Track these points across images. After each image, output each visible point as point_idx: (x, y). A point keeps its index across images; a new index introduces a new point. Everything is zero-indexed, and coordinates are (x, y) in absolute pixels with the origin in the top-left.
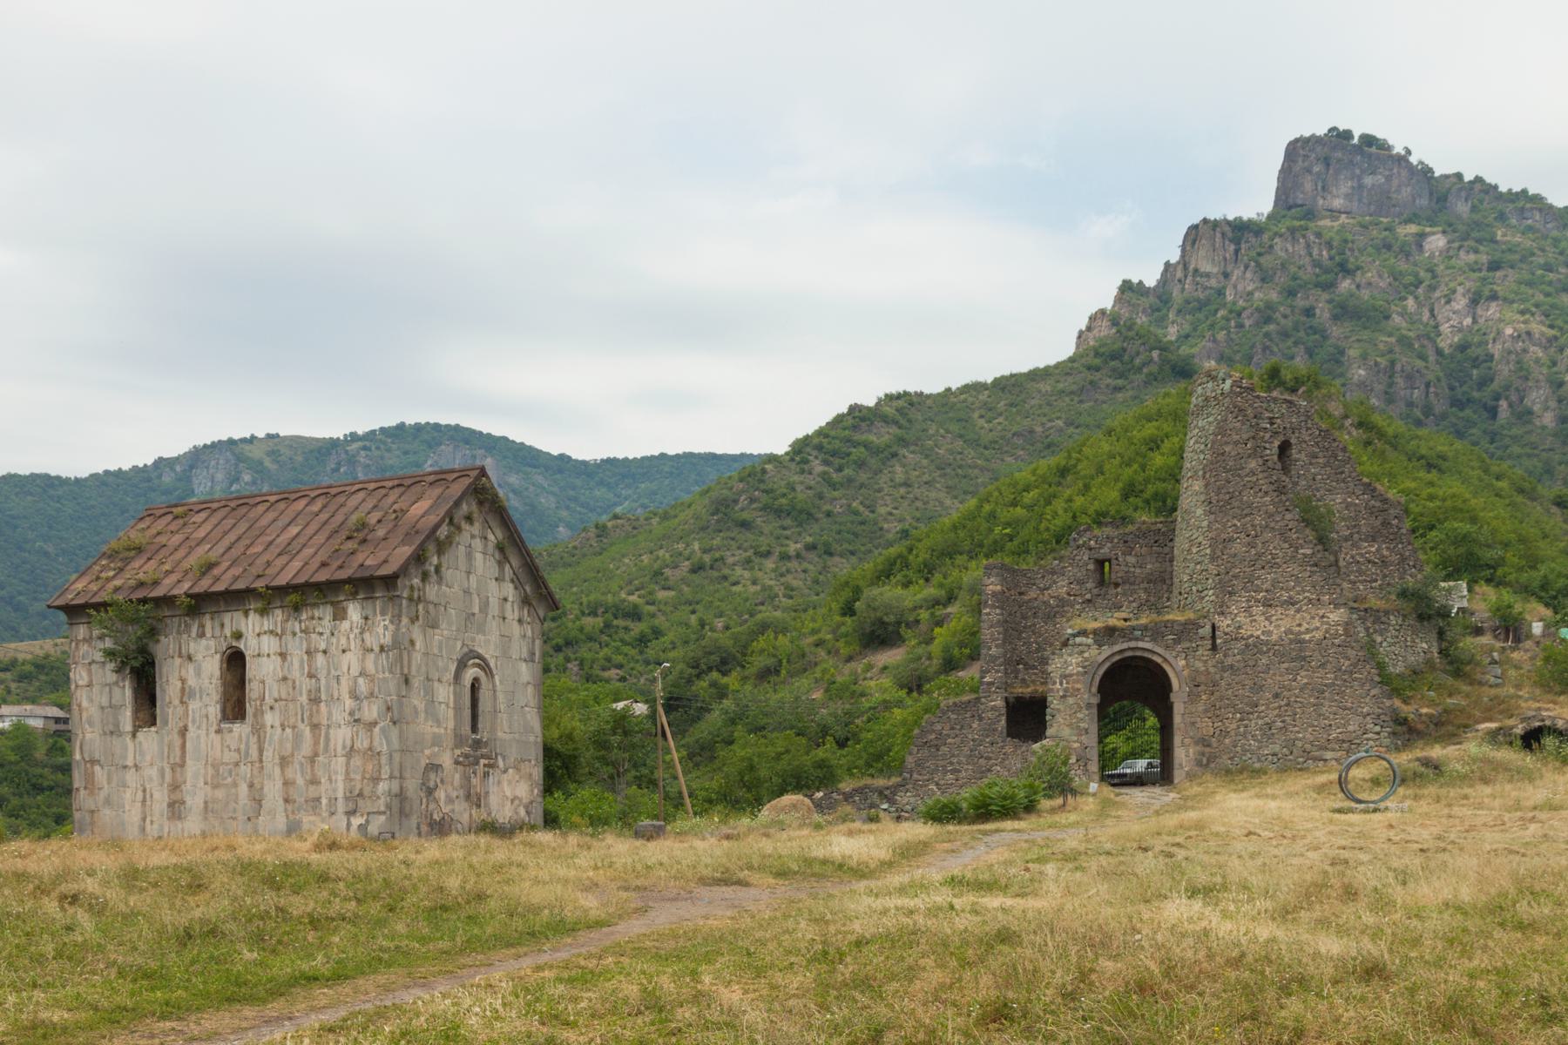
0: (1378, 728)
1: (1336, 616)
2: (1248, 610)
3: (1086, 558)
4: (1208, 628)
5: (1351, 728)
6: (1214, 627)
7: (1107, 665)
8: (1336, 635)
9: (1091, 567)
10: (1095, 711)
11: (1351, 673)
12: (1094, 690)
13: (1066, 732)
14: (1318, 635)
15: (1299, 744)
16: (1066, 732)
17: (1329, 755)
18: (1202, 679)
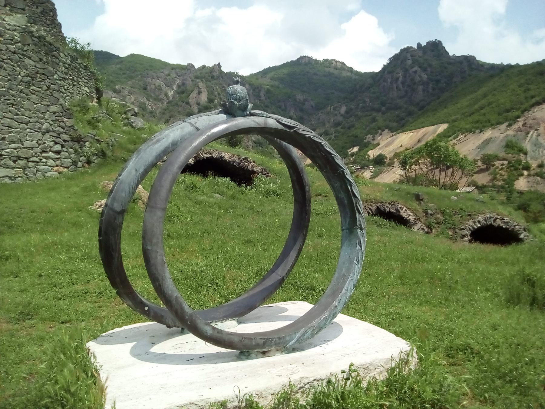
0: (58, 147)
5: (26, 144)
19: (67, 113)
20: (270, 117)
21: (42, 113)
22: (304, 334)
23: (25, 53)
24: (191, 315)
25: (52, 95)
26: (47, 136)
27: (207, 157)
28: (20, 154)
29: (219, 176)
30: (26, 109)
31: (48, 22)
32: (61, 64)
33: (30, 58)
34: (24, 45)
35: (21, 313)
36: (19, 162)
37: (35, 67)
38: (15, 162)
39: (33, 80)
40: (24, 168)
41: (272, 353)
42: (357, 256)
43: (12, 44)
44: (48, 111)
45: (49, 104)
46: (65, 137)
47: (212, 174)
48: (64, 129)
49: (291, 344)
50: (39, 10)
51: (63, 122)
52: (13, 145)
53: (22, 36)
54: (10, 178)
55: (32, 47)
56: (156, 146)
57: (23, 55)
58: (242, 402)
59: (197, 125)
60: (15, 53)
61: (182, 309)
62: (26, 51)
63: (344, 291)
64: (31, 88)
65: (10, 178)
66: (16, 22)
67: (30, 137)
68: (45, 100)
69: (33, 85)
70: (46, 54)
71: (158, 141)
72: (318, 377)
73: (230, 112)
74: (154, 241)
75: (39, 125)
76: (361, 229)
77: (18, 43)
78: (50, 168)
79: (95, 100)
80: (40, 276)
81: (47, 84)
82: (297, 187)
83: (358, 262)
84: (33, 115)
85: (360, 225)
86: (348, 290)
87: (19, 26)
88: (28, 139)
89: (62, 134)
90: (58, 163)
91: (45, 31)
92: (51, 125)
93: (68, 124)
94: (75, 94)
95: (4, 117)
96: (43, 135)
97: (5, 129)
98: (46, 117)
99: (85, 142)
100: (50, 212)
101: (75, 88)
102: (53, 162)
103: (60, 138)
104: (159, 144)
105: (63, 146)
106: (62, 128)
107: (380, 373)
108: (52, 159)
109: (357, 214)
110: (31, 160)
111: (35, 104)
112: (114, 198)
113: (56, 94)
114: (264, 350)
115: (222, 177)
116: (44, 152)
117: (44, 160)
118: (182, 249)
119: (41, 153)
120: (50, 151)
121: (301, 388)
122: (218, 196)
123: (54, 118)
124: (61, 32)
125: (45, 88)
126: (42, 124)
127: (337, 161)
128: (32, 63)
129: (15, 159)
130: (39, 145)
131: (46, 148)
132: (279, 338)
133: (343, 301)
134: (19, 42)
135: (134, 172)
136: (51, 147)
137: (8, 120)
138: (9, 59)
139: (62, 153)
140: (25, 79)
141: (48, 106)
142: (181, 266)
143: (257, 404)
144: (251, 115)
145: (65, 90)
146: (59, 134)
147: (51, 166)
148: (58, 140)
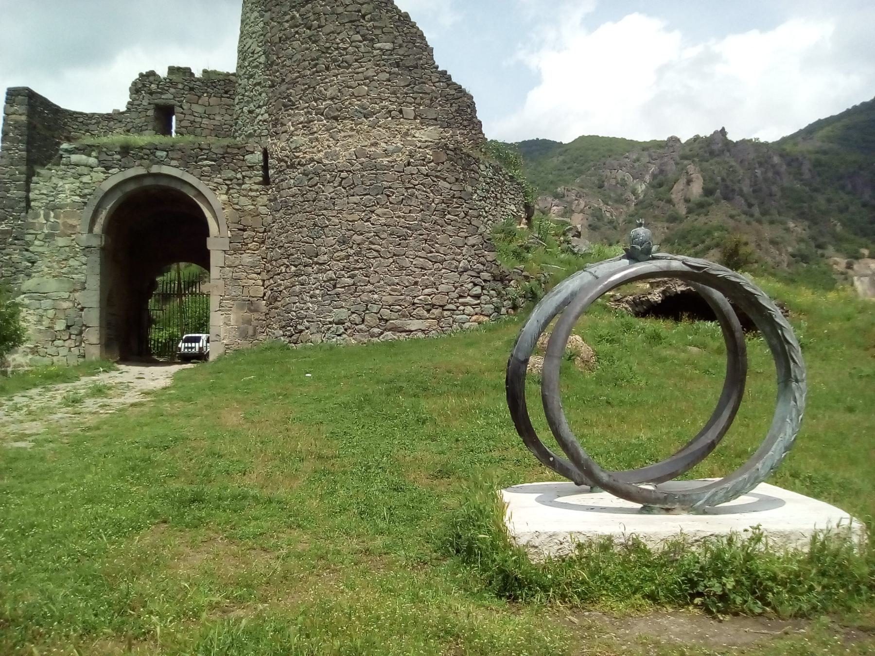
0: (477, 290)
1: (427, 134)
2: (307, 125)
3: (145, 103)
4: (258, 157)
5: (442, 288)
7: (118, 195)
8: (424, 161)
9: (151, 113)
10: (95, 258)
12: (97, 229)
13: (51, 285)
16: (51, 285)
17: (414, 324)
18: (248, 221)
19: (488, 244)
20: (675, 259)
21: (459, 248)
22: (714, 495)
23: (438, 174)
24: (586, 460)
26: (465, 275)
27: (682, 291)
28: (434, 301)
29: (699, 320)
30: (441, 245)
31: (465, 123)
32: (481, 179)
33: (445, 179)
34: (438, 164)
35: (440, 471)
36: (433, 311)
38: (428, 311)
40: (438, 319)
41: (676, 511)
42: (791, 414)
43: (424, 165)
45: (467, 235)
46: (486, 275)
47: (689, 317)
48: (484, 265)
49: (698, 504)
50: (453, 109)
52: (427, 291)
55: (447, 164)
56: (557, 297)
57: (437, 177)
58: (629, 540)
59: (596, 274)
60: (427, 175)
61: (578, 453)
63: (770, 453)
65: (423, 331)
66: (428, 137)
69: (449, 213)
70: (464, 169)
71: (558, 292)
72: (717, 533)
73: (633, 256)
74: (552, 387)
75: (455, 263)
76: (797, 381)
79: (524, 221)
80: (457, 440)
82: (727, 334)
83: (791, 420)
84: (449, 251)
85: (795, 376)
86: (776, 452)
88: (444, 281)
90: (478, 310)
91: (462, 134)
92: (469, 262)
94: (499, 216)
98: (464, 252)
99: (510, 281)
100: (468, 372)
101: (499, 208)
104: (559, 295)
105: (483, 288)
107: (803, 545)
108: (471, 305)
109: (792, 364)
110: (446, 308)
112: (518, 348)
113: (475, 222)
114: (667, 506)
115: (705, 320)
116: (461, 296)
117: (461, 308)
118: (623, 419)
119: (458, 298)
121: (697, 541)
122: (695, 349)
123: (473, 252)
124: (481, 132)
125: (462, 214)
126: (459, 262)
127: (761, 302)
128: (449, 186)
129: (429, 307)
130: (456, 288)
131: (464, 292)
132: (684, 496)
133: (769, 463)
134: (433, 161)
135: (536, 322)
139: (482, 297)
141: (466, 237)
142: (616, 439)
143: (645, 546)
144: (654, 258)
146: (479, 273)
148: (477, 280)
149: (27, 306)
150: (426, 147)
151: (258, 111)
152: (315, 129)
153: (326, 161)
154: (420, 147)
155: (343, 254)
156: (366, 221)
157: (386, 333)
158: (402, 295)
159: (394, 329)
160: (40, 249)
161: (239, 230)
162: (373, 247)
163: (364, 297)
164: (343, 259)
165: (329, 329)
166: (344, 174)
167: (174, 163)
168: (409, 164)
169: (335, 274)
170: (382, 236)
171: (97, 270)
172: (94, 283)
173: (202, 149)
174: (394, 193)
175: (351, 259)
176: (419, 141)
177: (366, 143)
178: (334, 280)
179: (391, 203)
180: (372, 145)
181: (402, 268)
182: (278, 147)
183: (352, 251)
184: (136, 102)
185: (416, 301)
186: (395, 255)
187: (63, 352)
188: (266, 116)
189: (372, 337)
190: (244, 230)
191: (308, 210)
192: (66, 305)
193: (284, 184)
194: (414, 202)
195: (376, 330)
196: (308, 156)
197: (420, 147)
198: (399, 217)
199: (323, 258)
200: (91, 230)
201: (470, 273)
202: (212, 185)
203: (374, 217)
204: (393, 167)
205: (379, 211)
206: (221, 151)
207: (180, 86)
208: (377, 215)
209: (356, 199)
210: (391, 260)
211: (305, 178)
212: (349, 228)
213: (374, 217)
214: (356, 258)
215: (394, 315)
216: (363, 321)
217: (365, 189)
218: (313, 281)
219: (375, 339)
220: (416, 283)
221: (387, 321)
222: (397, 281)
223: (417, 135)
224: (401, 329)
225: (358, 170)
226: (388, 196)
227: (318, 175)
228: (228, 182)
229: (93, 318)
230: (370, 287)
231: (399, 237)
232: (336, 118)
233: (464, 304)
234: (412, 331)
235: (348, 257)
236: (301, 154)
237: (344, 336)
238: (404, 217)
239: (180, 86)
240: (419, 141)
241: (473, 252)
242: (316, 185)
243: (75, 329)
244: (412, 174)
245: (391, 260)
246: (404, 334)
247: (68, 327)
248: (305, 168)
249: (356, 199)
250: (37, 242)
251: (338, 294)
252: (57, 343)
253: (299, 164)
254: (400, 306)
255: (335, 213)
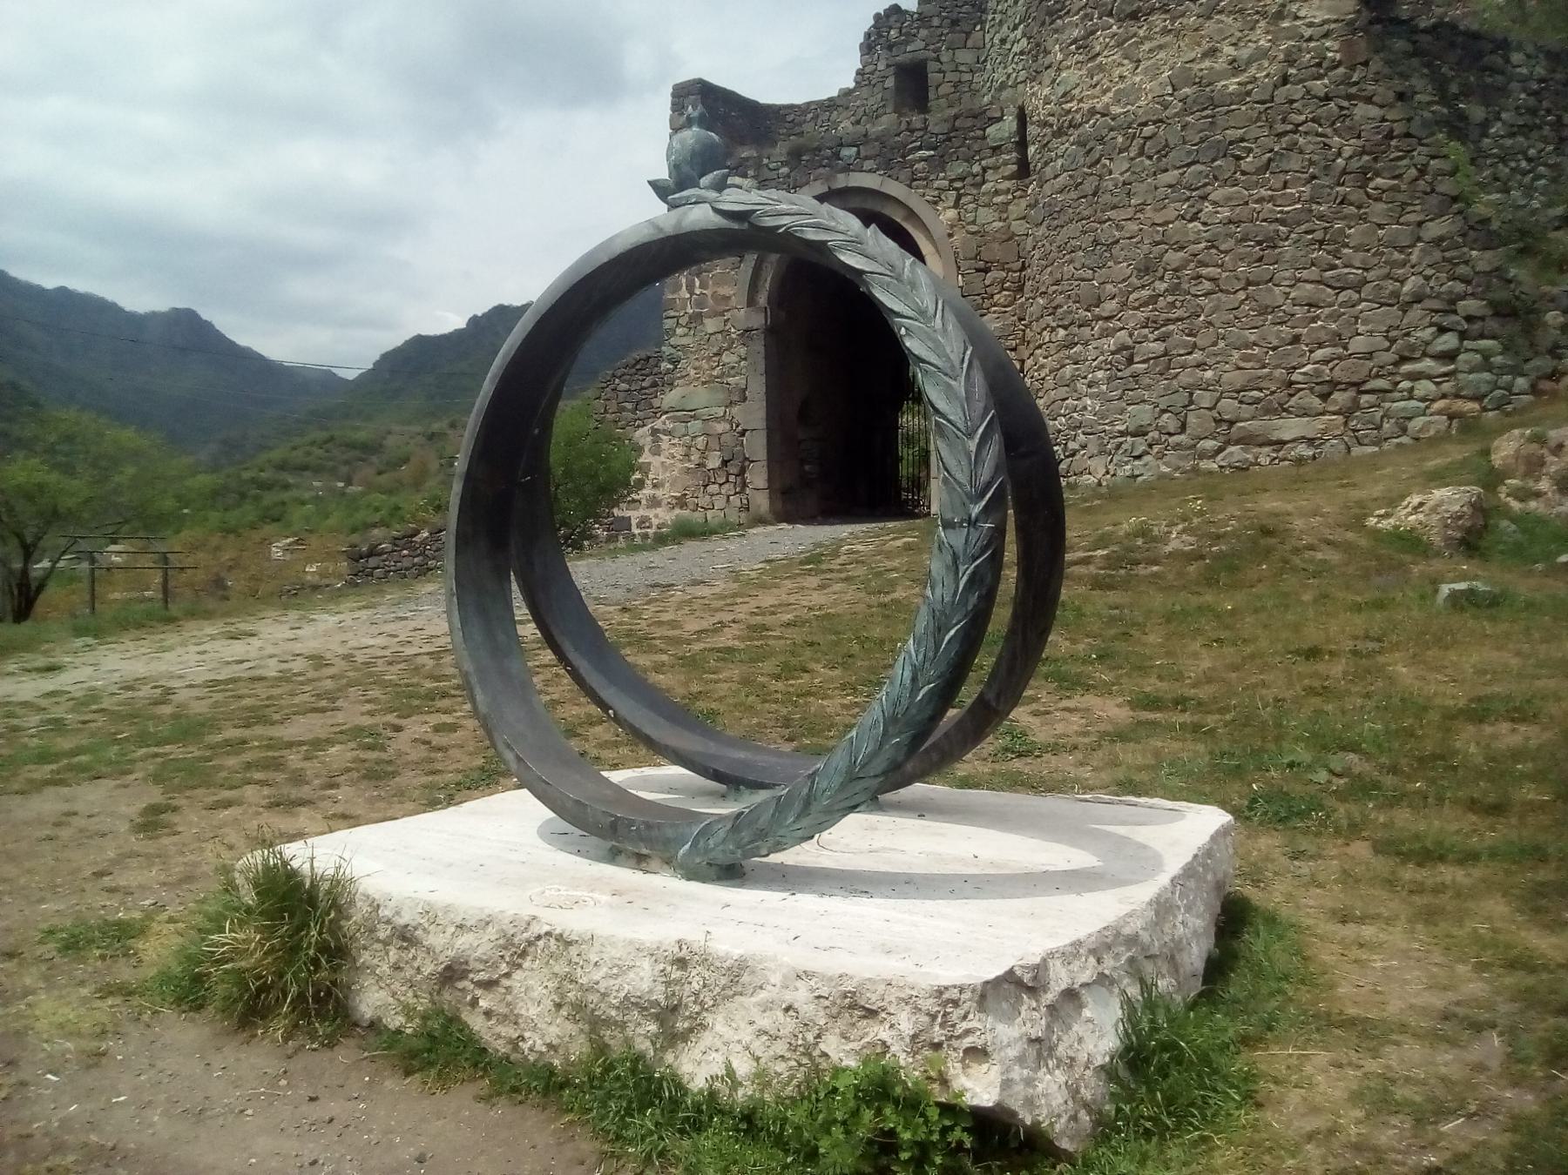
0: (1449, 341)
2: (1082, 44)
3: (881, 66)
4: (1009, 124)
5: (1358, 344)
6: (1022, 118)
8: (1321, 66)
10: (759, 346)
11: (1364, 176)
12: (762, 300)
13: (701, 397)
14: (1264, 72)
15: (1205, 399)
16: (701, 397)
17: (1290, 427)
18: (996, 251)
21: (1401, 250)
23: (1353, 90)
25: (1433, 191)
26: (1416, 312)
28: (1337, 373)
30: (1356, 249)
33: (1369, 100)
34: (1352, 68)
37: (1383, 120)
38: (1324, 397)
39: (1375, 160)
40: (1347, 413)
41: (654, 864)
43: (1319, 77)
44: (1419, 239)
45: (1421, 217)
46: (1471, 306)
48: (1468, 282)
51: (1466, 263)
52: (1320, 354)
53: (1347, 47)
54: (1310, 441)
57: (1349, 97)
60: (1327, 98)
62: (1356, 83)
64: (1372, 185)
65: (1310, 441)
66: (1330, 10)
67: (1365, 322)
68: (1410, 208)
69: (1377, 174)
75: (1391, 286)
77: (1336, 67)
78: (1423, 405)
81: (1422, 159)
87: (1336, 21)
88: (1361, 329)
89: (1463, 298)
90: (1446, 387)
92: (1427, 278)
93: (1482, 266)
95: (1299, 280)
96: (1405, 312)
97: (1300, 312)
102: (1432, 387)
103: (1455, 312)
105: (1463, 336)
106: (1462, 281)
108: (1430, 377)
110: (1367, 387)
111: (1381, 226)
116: (1404, 359)
117: (1405, 384)
119: (1396, 364)
120: (1425, 354)
126: (1402, 282)
128: (1374, 111)
129: (1325, 389)
130: (1393, 341)
131: (1412, 348)
132: (649, 826)
134: (1340, 63)
136: (1427, 343)
137: (1308, 286)
138: (1313, 120)
139: (1462, 357)
140: (1355, 164)
141: (1420, 224)
145: (1529, 160)
147: (1423, 400)
148: (1447, 321)
149: (669, 433)
150: (1326, 35)
151: (1012, 36)
152: (1098, 48)
153: (1116, 110)
154: (1310, 39)
155: (1146, 293)
156: (1191, 221)
157: (1231, 449)
158: (1264, 367)
159: (1247, 440)
160: (684, 341)
161: (978, 270)
162: (1204, 271)
163: (1186, 378)
164: (1145, 304)
165: (1119, 446)
166: (1148, 130)
167: (868, 164)
168: (1285, 80)
169: (1131, 335)
170: (1223, 247)
171: (762, 367)
172: (758, 389)
173: (912, 131)
174: (1250, 150)
175: (1161, 302)
176: (1310, 25)
177: (1193, 55)
178: (1126, 348)
179: (1244, 173)
180: (1205, 55)
181: (1264, 311)
182: (1039, 98)
183: (1161, 286)
184: (868, 70)
185: (1295, 377)
186: (1249, 283)
187: (720, 502)
188: (1024, 41)
189: (1201, 458)
190: (986, 271)
191: (1086, 213)
192: (721, 427)
193: (1048, 169)
194: (1295, 162)
195: (1210, 444)
196: (1085, 106)
197: (1310, 39)
198: (1260, 200)
199: (1110, 306)
200: (751, 302)
201: (1429, 304)
202: (931, 194)
203: (1208, 208)
204: (1249, 93)
205: (1218, 194)
206: (945, 127)
207: (936, 22)
208: (1214, 203)
209: (1171, 176)
210: (1242, 295)
211: (1082, 151)
212: (1158, 238)
213: (1208, 208)
214: (1170, 299)
215: (1247, 411)
216: (1183, 428)
217: (1189, 153)
218: (1092, 354)
219: (1205, 465)
220: (1296, 339)
221: (1231, 423)
222: (1253, 338)
223: (1302, 13)
224: (1260, 440)
225: (1176, 115)
226: (1238, 158)
227: (1101, 140)
228: (958, 185)
229: (757, 446)
230: (1197, 356)
231: (1259, 243)
232: (1134, 16)
233: (1415, 377)
234: (1285, 443)
235: (1153, 299)
236: (1073, 105)
237: (1147, 458)
238: (1271, 199)
239: (936, 22)
240: (1310, 25)
241: (1437, 255)
242: (1098, 161)
243: (735, 466)
244: (1292, 102)
245: (1242, 295)
246: (1267, 449)
247: (725, 463)
248: (1081, 130)
249: (1171, 176)
250: (679, 331)
251: (1134, 376)
252: (713, 488)
253: (1070, 126)
254: (1261, 390)
255: (1129, 212)
